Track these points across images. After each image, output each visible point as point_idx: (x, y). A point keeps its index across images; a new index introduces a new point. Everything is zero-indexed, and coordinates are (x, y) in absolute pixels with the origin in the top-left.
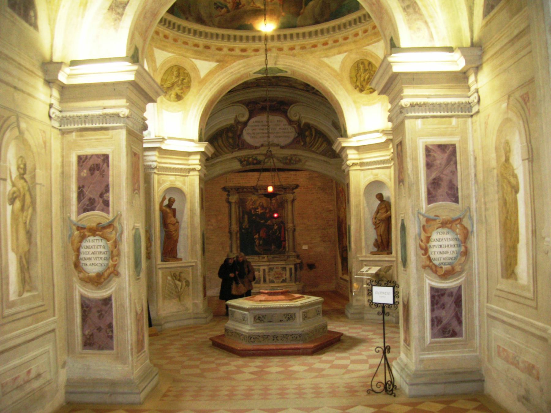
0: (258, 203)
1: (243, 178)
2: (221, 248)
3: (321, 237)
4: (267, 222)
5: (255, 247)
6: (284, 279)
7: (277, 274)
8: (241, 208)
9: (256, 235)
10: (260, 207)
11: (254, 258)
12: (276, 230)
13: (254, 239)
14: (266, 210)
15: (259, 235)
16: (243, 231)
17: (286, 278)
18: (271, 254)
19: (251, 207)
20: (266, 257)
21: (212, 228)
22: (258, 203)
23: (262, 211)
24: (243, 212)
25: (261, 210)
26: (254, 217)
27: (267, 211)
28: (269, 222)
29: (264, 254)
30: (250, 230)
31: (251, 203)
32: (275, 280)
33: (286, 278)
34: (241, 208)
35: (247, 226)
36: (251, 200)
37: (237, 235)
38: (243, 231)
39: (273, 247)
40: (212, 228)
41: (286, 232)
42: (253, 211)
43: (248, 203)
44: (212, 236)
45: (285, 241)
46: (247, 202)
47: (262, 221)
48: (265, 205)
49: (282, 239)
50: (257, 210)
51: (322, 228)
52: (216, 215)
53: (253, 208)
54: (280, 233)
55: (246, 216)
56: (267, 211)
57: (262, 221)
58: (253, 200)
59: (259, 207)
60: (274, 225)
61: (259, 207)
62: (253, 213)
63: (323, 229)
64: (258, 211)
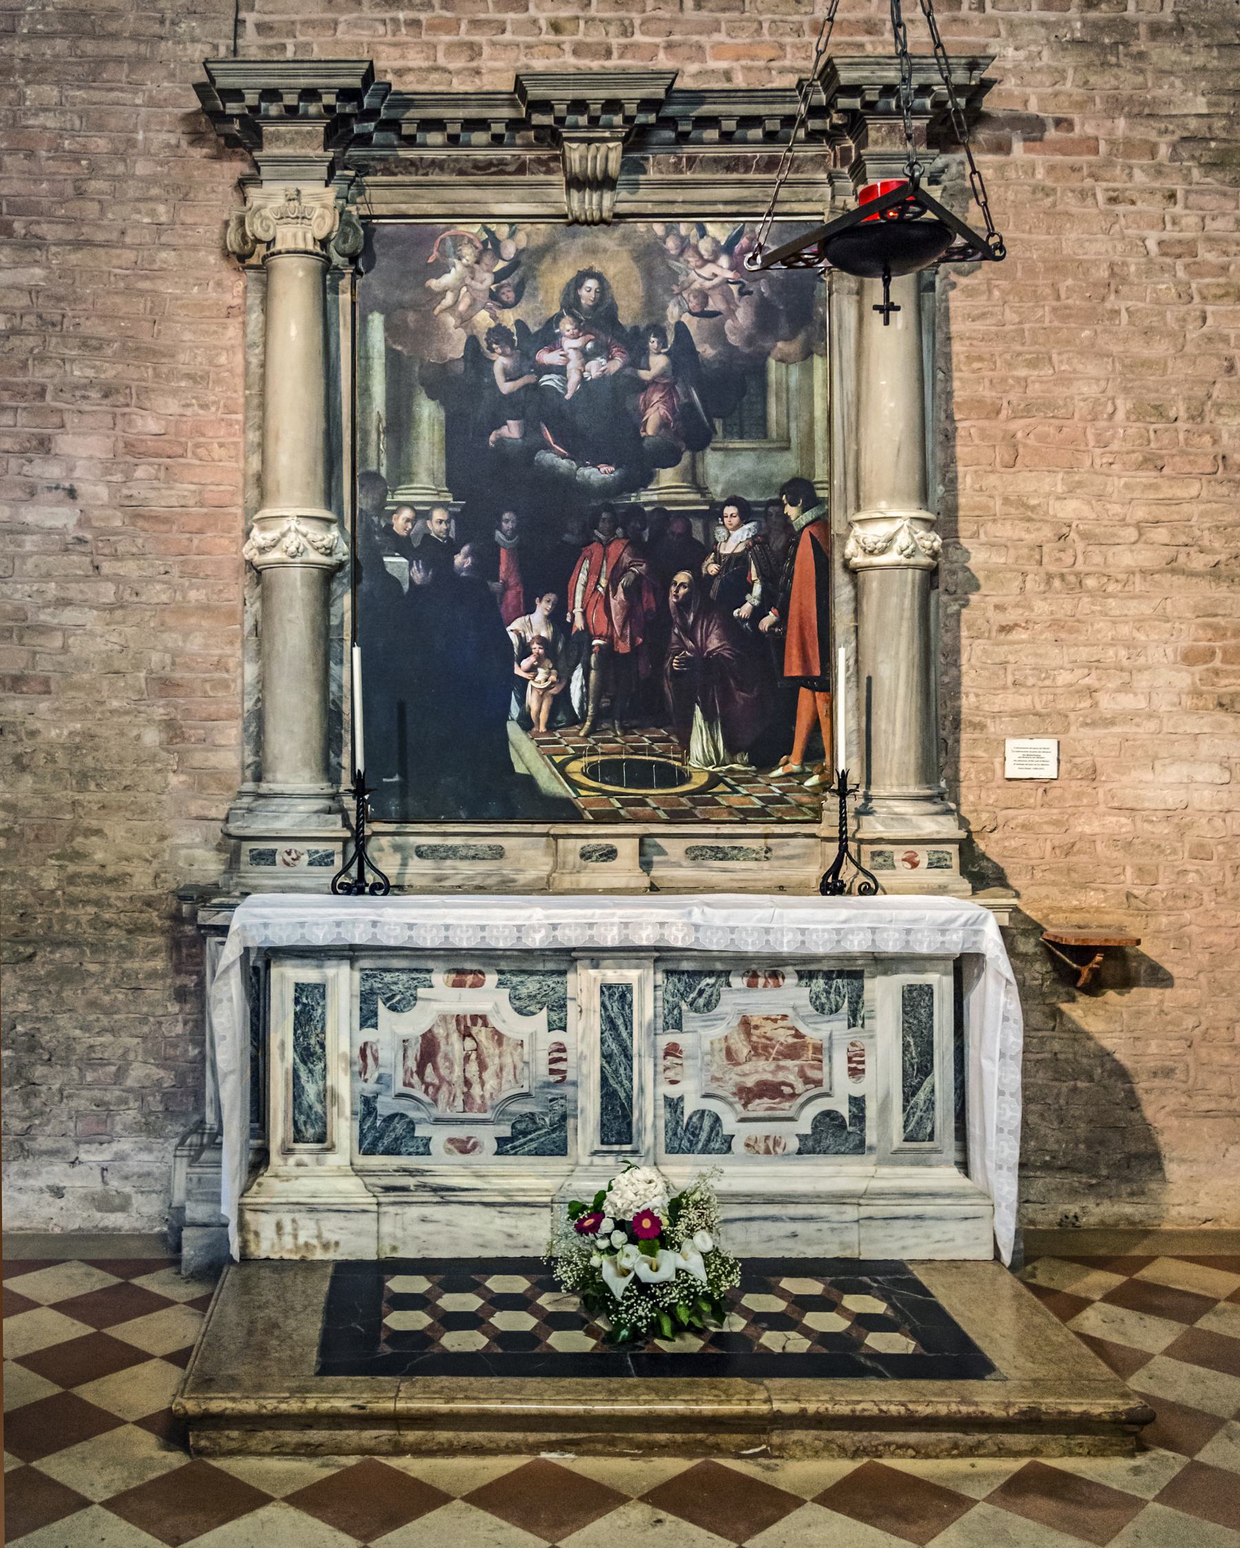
0: (555, 279)
1: (415, 24)
2: (152, 737)
3: (1190, 658)
4: (645, 479)
5: (513, 730)
6: (844, 1110)
7: (760, 1050)
8: (377, 321)
9: (530, 610)
10: (582, 328)
11: (499, 853)
12: (737, 563)
13: (506, 655)
14: (638, 357)
15: (557, 618)
16: (395, 563)
17: (857, 1103)
18: (677, 817)
19: (483, 319)
20: (628, 849)
21: (63, 517)
22: (555, 279)
23: (595, 368)
24: (394, 362)
25: (586, 356)
26: (512, 430)
27: (658, 362)
28: (667, 476)
29: (601, 818)
30: (461, 560)
31: (486, 281)
32: (729, 1124)
33: (857, 1103)
34: (377, 321)
35: (438, 523)
36: (492, 245)
37: (326, 601)
38: (395, 563)
39: (700, 742)
40: (63, 517)
41: (842, 591)
42: (501, 363)
43: (447, 279)
44: (64, 603)
45: (824, 684)
46: (441, 269)
47: (598, 474)
48: (628, 312)
49: (793, 668)
50: (548, 357)
51: (1199, 562)
52: (108, 392)
53: (499, 334)
54: (776, 597)
55: (428, 413)
56: (658, 362)
57: (598, 474)
58: (509, 250)
59: (567, 326)
60: (714, 514)
61: (567, 326)
62: (506, 387)
63: (1215, 573)
64: (561, 370)
